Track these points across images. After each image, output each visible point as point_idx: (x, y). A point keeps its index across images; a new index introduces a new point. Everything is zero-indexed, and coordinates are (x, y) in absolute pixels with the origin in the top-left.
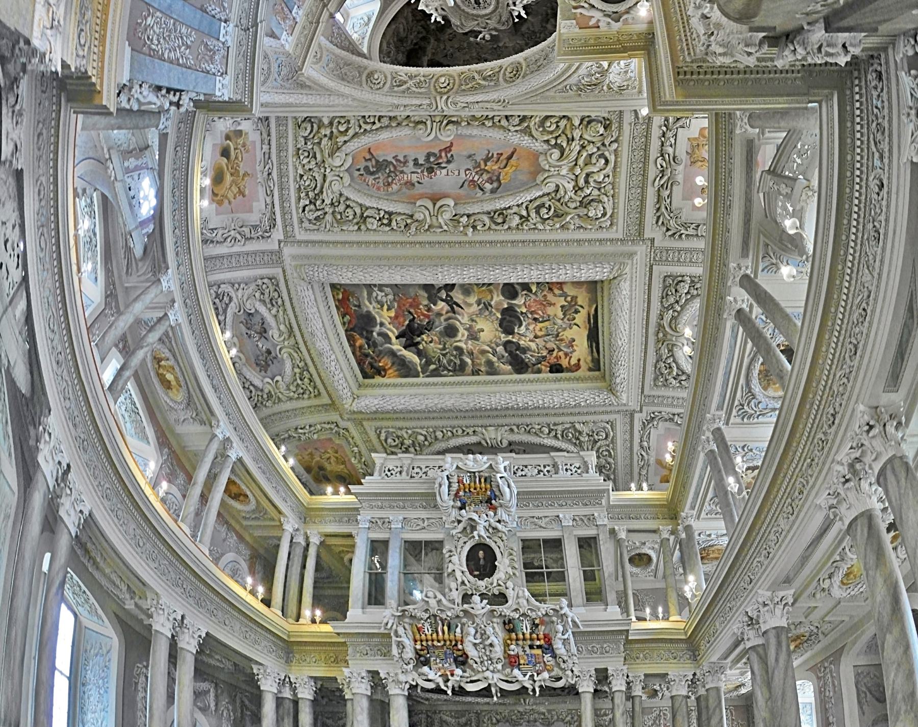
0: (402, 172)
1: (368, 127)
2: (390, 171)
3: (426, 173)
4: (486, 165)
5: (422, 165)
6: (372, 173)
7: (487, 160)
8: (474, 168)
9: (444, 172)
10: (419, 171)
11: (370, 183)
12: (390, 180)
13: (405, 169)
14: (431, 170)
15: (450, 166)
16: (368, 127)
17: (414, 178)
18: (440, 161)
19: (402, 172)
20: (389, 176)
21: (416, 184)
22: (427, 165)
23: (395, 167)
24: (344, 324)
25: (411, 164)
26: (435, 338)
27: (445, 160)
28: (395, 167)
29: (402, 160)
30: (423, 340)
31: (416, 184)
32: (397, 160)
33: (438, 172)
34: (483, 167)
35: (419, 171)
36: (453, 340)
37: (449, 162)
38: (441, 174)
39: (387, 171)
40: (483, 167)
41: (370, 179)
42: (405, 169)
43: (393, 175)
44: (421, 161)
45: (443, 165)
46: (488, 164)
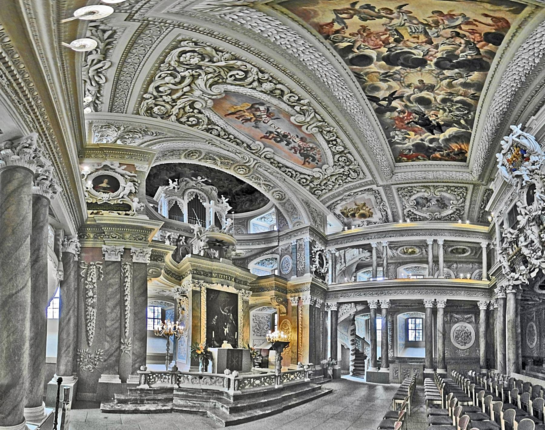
9: (279, 130)
15: (273, 130)
24: (425, 160)
26: (432, 112)
30: (434, 120)
33: (282, 133)
36: (433, 102)
37: (271, 132)
38: (282, 131)
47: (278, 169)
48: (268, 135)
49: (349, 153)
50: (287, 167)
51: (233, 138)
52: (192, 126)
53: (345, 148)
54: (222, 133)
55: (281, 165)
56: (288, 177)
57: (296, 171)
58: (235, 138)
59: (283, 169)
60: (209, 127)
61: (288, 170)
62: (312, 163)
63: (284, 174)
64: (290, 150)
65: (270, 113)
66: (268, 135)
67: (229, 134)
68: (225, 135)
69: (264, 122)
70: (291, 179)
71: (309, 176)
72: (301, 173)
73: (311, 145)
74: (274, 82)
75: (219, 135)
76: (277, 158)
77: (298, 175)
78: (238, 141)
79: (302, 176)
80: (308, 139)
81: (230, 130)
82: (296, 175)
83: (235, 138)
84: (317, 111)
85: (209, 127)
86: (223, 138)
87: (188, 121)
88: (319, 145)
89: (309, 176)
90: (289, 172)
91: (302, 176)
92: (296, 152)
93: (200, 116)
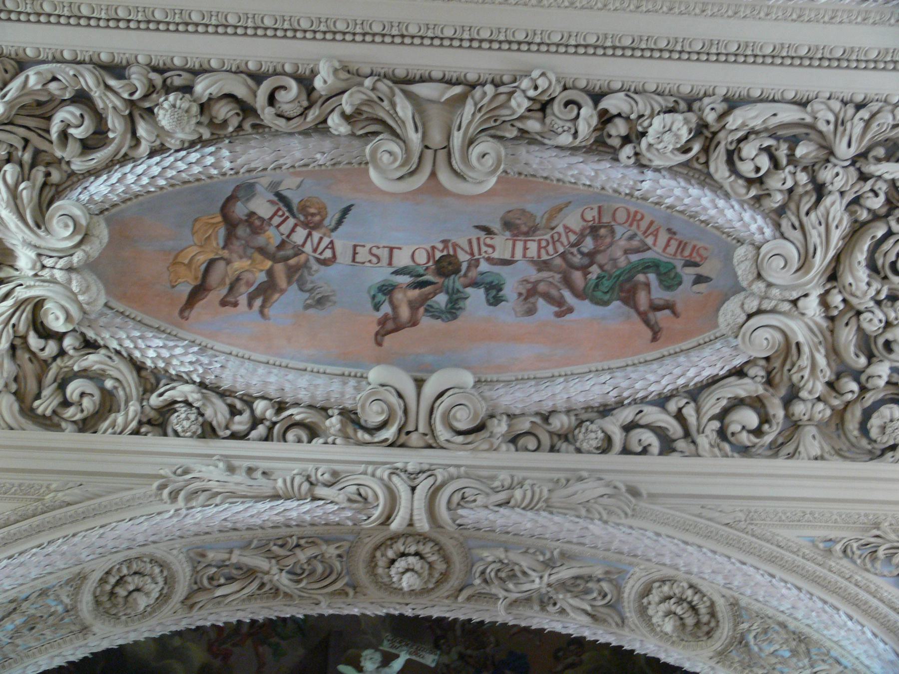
0: (543, 265)
1: (653, 415)
2: (584, 269)
3: (463, 257)
4: (270, 273)
5: (475, 284)
6: (654, 266)
7: (266, 291)
8: (306, 265)
9: (402, 259)
10: (484, 266)
11: (663, 237)
12: (589, 244)
13: (533, 274)
14: (446, 266)
15: (381, 274)
16: (653, 415)
17: (502, 246)
18: (414, 293)
19: (543, 265)
20: (591, 256)
21: (496, 226)
22: (456, 282)
23: (568, 282)
25: (510, 290)
27: (398, 296)
28: (568, 282)
29: (541, 303)
31: (496, 226)
32: (559, 302)
33: (421, 258)
34: (280, 268)
35: (484, 266)
37: (387, 290)
38: (414, 251)
39: (595, 271)
40: (280, 268)
41: (658, 249)
42: (533, 274)
43: (577, 259)
44: (476, 297)
45: (405, 280)
46: (262, 277)
47: (566, 459)
48: (386, 309)
49: (732, 103)
50: (605, 411)
51: (269, 413)
52: (87, 425)
53: (691, 103)
54: (217, 411)
55: (559, 422)
56: (655, 462)
57: (662, 401)
58: (281, 407)
59: (591, 437)
60: (155, 400)
61: (613, 426)
62: (677, 296)
63: (613, 460)
64: (531, 311)
65: (303, 208)
66: (386, 309)
67: (248, 401)
68: (234, 412)
69: (324, 262)
70: (673, 460)
71: (739, 372)
72: (695, 393)
73: (573, 220)
74: (177, 82)
75: (208, 431)
76: (512, 398)
77: (689, 412)
78: (298, 414)
79: (713, 403)
80: (530, 207)
81: (237, 375)
82: (679, 416)
83: (281, 407)
84: (401, 73)
85: (155, 400)
86: (234, 436)
87: (66, 404)
88: (599, 197)
89: (739, 372)
90: (628, 428)
91: (713, 403)
92: (563, 310)
93: (93, 360)
